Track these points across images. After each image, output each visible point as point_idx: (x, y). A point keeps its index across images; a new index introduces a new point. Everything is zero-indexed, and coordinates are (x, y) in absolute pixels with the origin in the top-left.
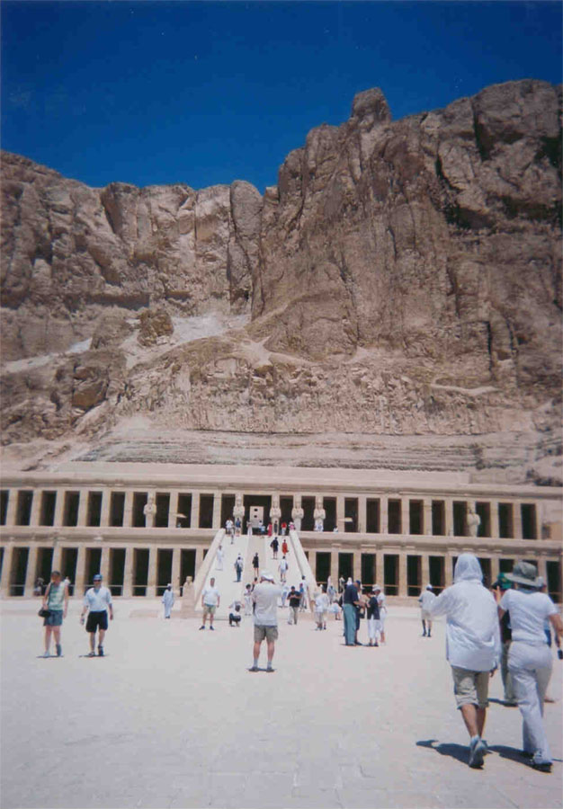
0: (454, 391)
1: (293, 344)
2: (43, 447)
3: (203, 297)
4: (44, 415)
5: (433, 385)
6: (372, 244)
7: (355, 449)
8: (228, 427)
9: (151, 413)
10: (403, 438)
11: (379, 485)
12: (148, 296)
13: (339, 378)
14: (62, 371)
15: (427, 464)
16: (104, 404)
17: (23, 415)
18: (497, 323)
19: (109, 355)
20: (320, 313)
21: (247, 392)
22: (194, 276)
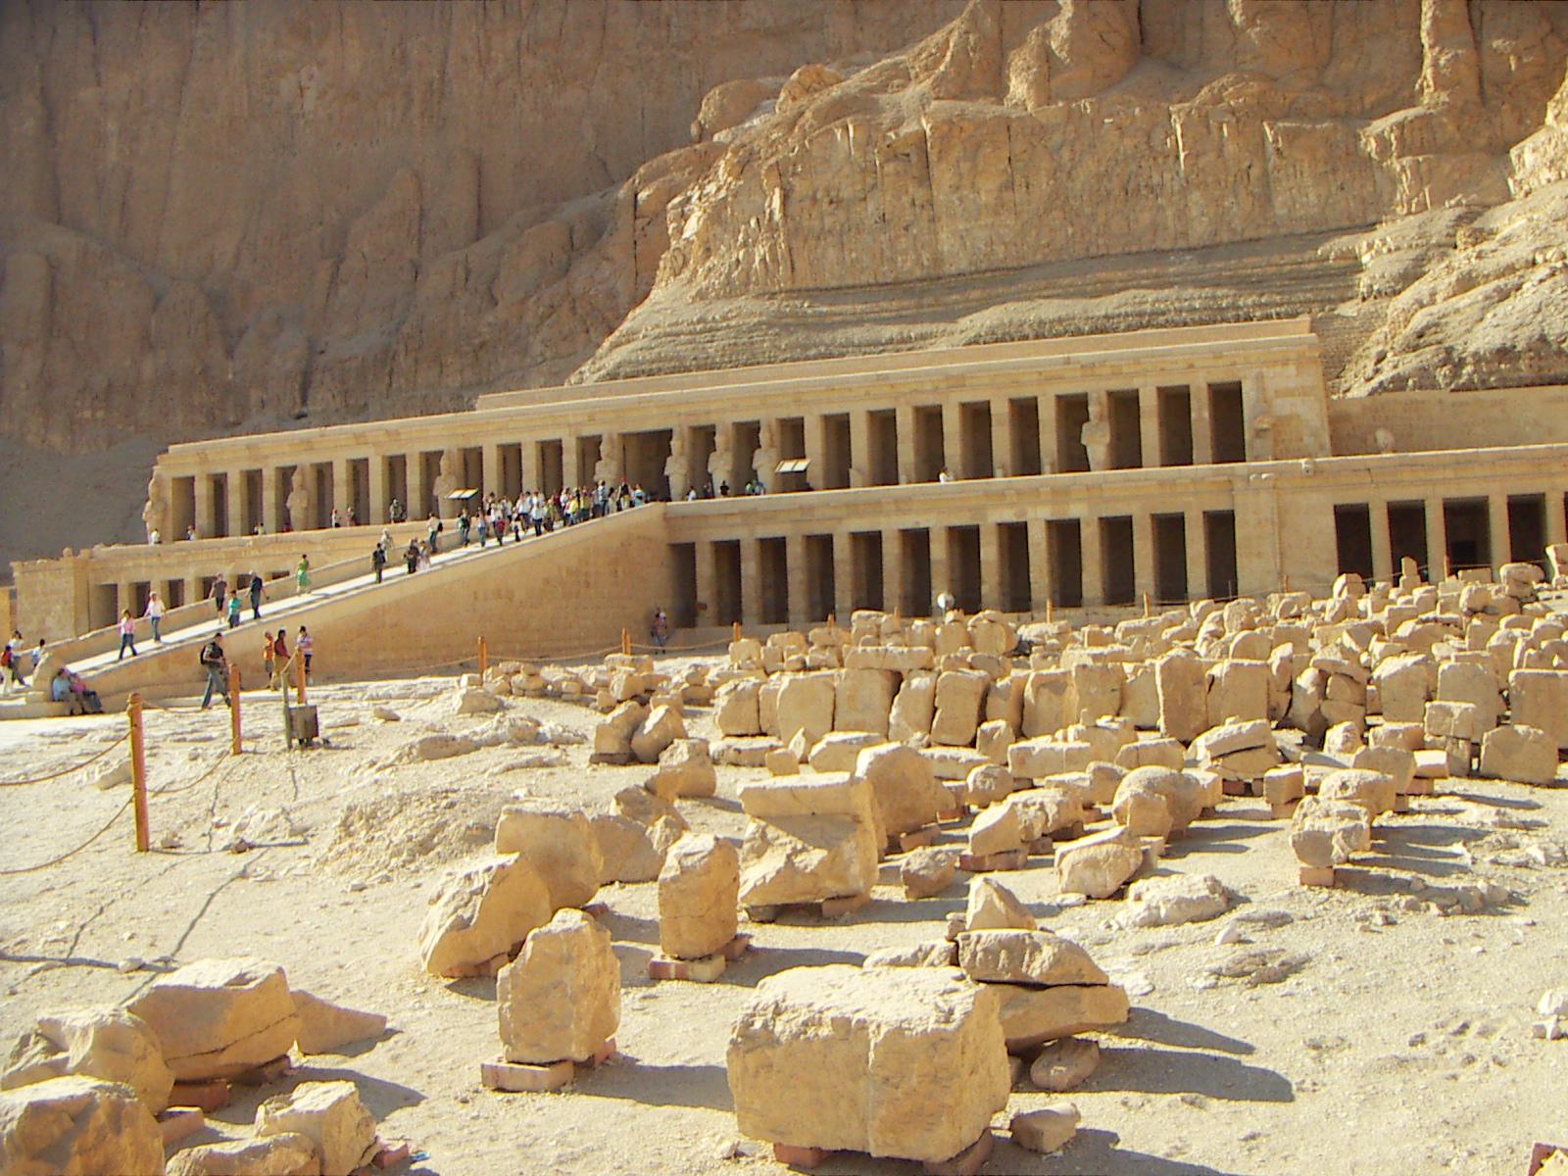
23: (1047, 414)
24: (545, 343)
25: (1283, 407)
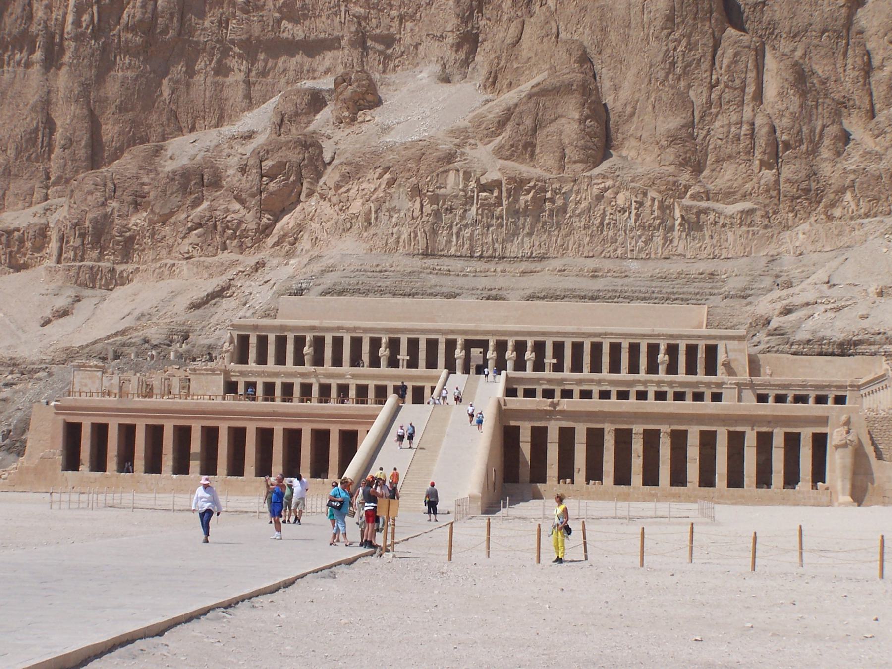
0: (708, 208)
1: (526, 149)
2: (234, 263)
3: (417, 39)
4: (228, 221)
5: (686, 201)
7: (594, 277)
8: (453, 251)
9: (365, 234)
10: (650, 263)
11: (583, 331)
12: (339, 39)
13: (578, 192)
14: (246, 165)
15: (670, 293)
16: (299, 208)
17: (203, 222)
18: (761, 126)
19: (305, 146)
20: (560, 111)
21: (474, 208)
22: (403, 11)
23: (644, 350)
24: (194, 245)
25: (732, 356)
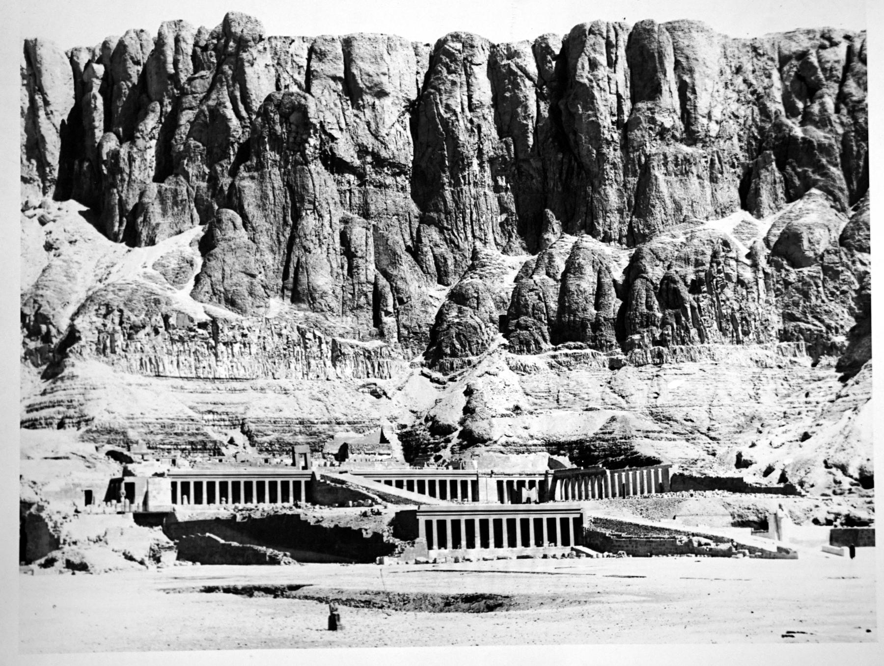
6: (271, 197)
